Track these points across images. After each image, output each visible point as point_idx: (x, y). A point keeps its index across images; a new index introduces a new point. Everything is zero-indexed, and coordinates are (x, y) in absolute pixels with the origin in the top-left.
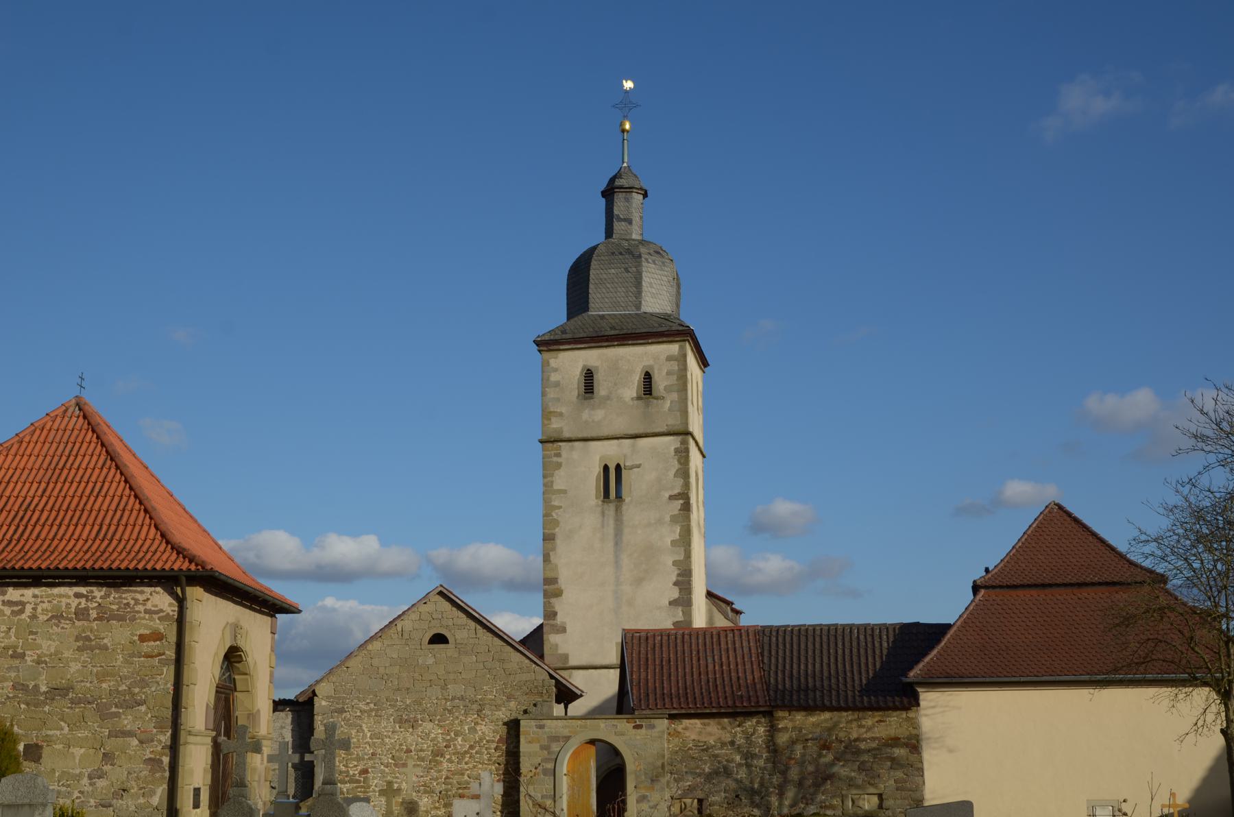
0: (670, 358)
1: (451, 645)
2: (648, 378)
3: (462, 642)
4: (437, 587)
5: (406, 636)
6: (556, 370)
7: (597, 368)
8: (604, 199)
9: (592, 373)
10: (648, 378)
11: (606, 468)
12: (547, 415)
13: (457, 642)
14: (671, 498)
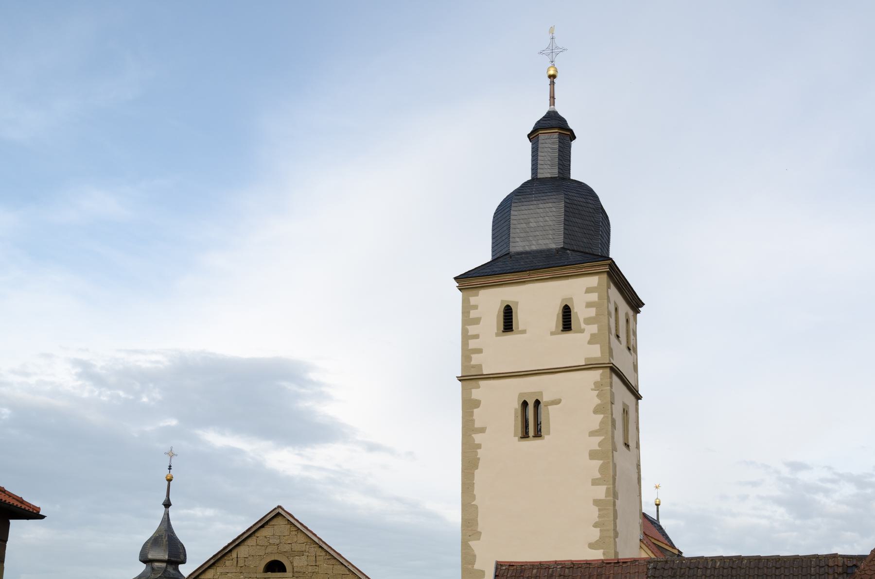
0: (589, 290)
1: (289, 574)
2: (567, 313)
3: (301, 570)
4: (275, 509)
5: (241, 563)
6: (475, 307)
7: (517, 303)
8: (531, 143)
9: (511, 309)
10: (567, 313)
11: (525, 404)
12: (467, 354)
13: (295, 570)
14: (592, 434)
